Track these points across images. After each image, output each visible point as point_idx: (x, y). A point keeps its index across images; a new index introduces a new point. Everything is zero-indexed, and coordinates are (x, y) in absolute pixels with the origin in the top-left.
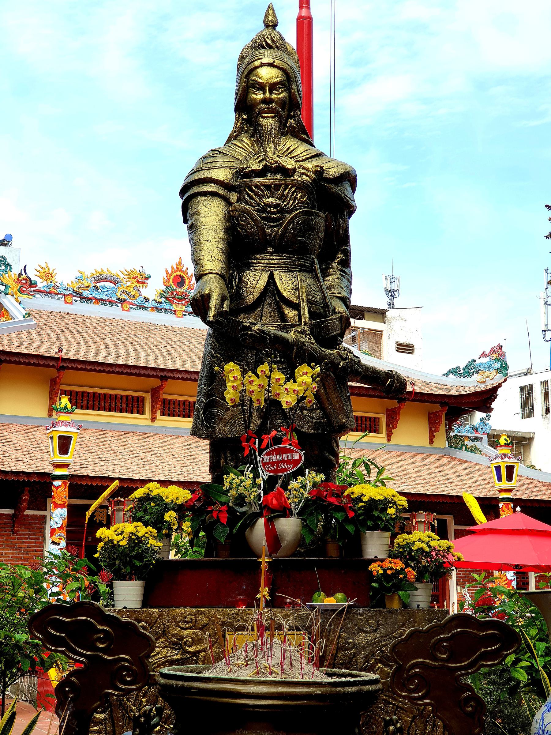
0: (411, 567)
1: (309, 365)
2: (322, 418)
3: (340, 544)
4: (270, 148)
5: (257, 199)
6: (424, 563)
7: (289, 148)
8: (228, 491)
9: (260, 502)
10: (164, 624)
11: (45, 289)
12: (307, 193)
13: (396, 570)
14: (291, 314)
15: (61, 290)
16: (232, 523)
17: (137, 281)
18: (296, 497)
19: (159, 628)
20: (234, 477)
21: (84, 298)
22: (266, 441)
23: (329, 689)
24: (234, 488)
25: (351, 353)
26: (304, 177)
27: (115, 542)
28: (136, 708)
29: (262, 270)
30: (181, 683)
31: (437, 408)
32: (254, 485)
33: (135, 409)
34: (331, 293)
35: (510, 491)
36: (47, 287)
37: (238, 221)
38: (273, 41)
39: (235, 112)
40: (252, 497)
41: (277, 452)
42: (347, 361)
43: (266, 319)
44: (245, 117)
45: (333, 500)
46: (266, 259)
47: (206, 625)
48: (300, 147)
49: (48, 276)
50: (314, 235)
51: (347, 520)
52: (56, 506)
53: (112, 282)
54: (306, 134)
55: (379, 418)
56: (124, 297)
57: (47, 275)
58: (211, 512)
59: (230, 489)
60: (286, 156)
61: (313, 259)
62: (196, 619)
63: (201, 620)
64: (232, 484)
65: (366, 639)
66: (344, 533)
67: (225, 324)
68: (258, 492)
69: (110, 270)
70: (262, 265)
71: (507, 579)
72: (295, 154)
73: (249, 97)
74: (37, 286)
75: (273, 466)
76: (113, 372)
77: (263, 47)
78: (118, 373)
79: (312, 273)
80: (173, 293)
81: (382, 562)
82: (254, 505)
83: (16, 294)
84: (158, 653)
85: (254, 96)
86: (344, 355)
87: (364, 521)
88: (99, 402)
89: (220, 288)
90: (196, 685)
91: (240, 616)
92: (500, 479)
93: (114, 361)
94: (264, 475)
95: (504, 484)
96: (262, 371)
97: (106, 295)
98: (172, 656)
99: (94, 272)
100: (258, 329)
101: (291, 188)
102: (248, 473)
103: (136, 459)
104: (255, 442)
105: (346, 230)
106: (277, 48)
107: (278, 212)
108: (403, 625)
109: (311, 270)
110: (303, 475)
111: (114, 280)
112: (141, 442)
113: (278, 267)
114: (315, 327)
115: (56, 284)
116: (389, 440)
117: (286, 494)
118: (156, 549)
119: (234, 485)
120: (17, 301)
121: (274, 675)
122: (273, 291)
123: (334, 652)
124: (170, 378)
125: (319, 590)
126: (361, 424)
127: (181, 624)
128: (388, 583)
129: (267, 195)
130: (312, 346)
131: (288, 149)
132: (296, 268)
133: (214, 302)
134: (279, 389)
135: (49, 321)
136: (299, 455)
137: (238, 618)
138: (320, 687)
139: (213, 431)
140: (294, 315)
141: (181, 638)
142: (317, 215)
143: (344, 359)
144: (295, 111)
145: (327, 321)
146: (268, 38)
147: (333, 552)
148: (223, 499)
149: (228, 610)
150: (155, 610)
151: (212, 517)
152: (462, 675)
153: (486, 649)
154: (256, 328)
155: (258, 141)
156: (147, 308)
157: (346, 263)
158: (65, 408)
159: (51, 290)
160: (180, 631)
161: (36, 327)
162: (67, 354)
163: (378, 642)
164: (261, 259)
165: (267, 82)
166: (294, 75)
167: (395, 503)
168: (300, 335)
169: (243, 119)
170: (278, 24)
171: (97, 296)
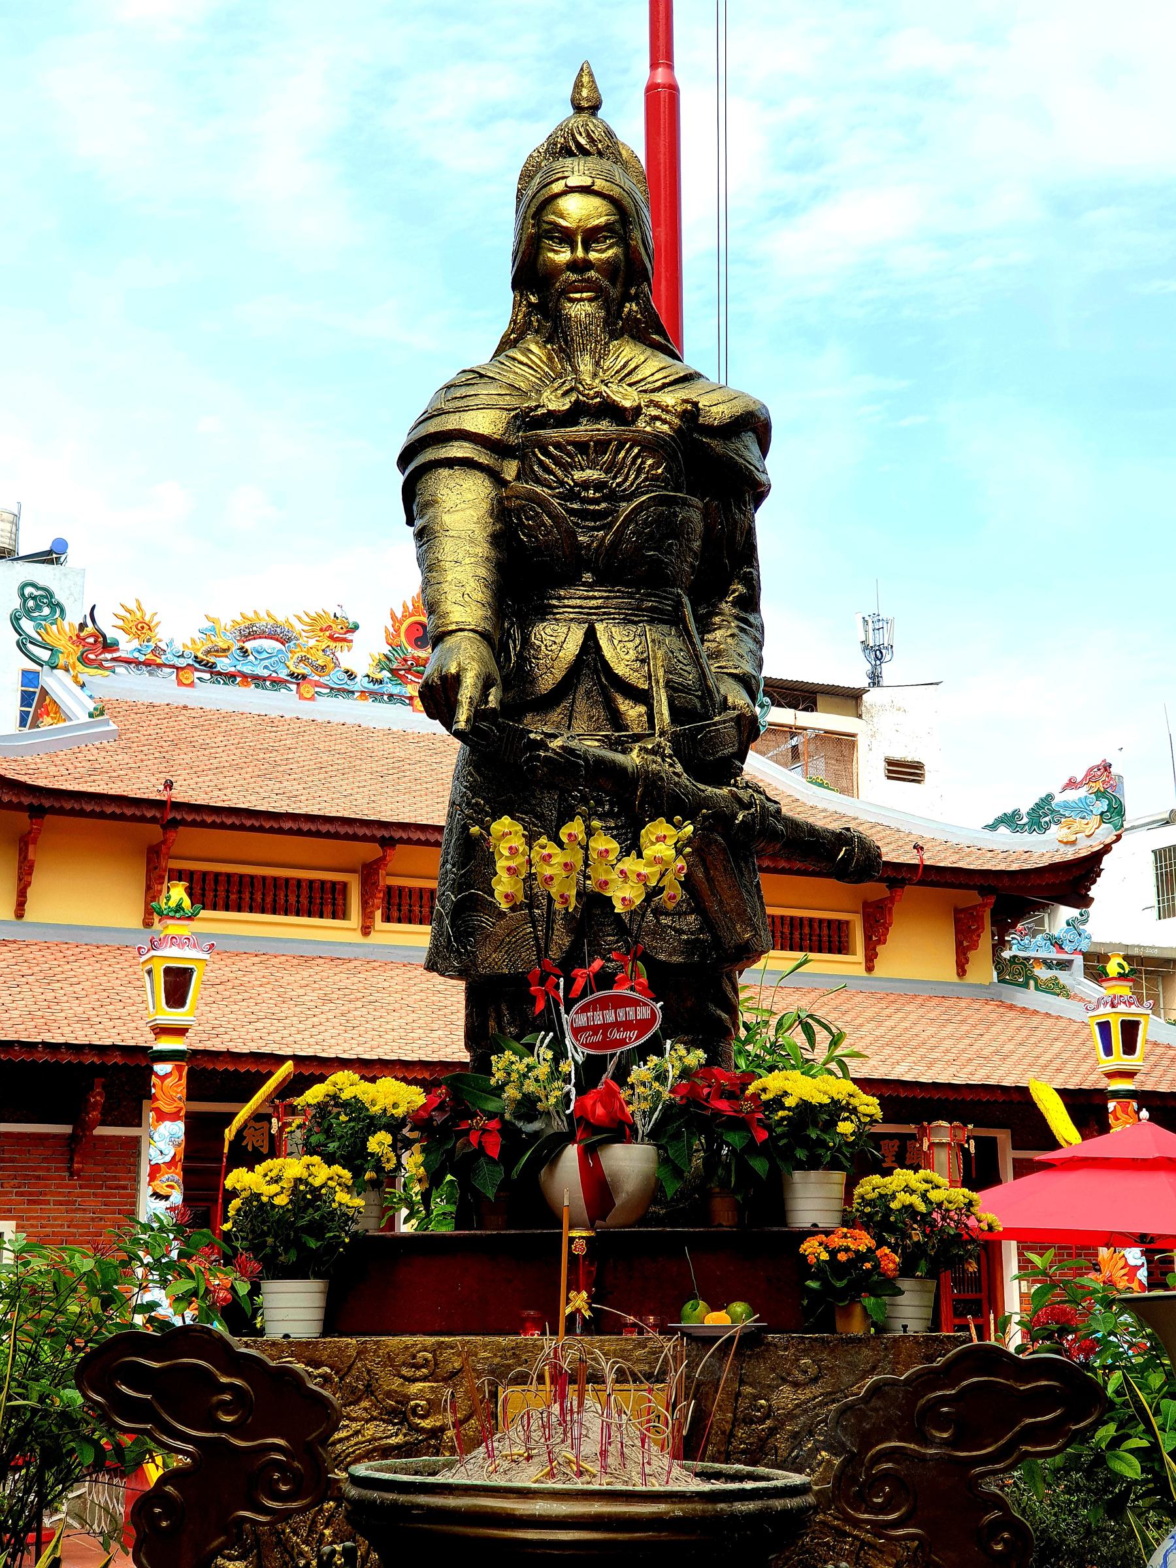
0: (889, 1245)
1: (670, 821)
2: (701, 931)
3: (739, 1198)
4: (585, 365)
5: (559, 473)
6: (917, 1236)
7: (627, 362)
8: (501, 1088)
9: (568, 1112)
10: (369, 1371)
11: (136, 655)
12: (663, 458)
13: (857, 1252)
14: (632, 712)
15: (170, 656)
16: (509, 1157)
17: (331, 637)
18: (645, 1099)
19: (357, 1379)
20: (513, 1058)
21: (219, 673)
22: (580, 983)
23: (699, 1507)
24: (514, 1082)
25: (760, 793)
26: (658, 424)
27: (265, 1199)
28: (312, 1549)
29: (572, 620)
30: (391, 1496)
31: (972, 898)
32: (555, 1074)
34: (719, 667)
35: (1129, 1075)
36: (139, 651)
37: (519, 519)
38: (592, 140)
39: (514, 287)
40: (552, 1101)
41: (603, 1004)
42: (753, 810)
43: (580, 725)
44: (533, 299)
45: (723, 1105)
46: (579, 598)
47: (457, 1373)
48: (649, 362)
49: (142, 628)
50: (681, 545)
51: (751, 1148)
52: (161, 1116)
53: (277, 640)
54: (661, 331)
55: (847, 922)
56: (302, 669)
57: (140, 625)
58: (466, 1133)
59: (505, 1084)
60: (620, 381)
61: (679, 595)
62: (435, 1360)
63: (448, 1361)
64: (509, 1074)
65: (796, 1399)
66: (746, 1172)
67: (495, 735)
68: (566, 1090)
69: (272, 612)
70: (572, 610)
71: (1126, 1265)
72: (640, 377)
73: (541, 258)
74: (118, 650)
75: (595, 1034)
76: (280, 831)
77: (571, 154)
78: (290, 832)
79: (677, 626)
80: (405, 660)
81: (827, 1236)
82: (557, 1117)
83: (74, 667)
84: (357, 1433)
85: (551, 255)
86: (746, 799)
87: (790, 1148)
88: (252, 894)
89: (481, 661)
90: (422, 1499)
91: (528, 1352)
92: (1108, 1051)
93: (282, 806)
94: (576, 1053)
95: (1119, 1060)
96: (570, 835)
97: (266, 667)
98: (386, 1437)
99: (239, 619)
100: (562, 747)
101: (631, 448)
102: (542, 1050)
103: (330, 1015)
104: (558, 984)
105: (750, 532)
106: (600, 154)
107: (604, 499)
108: (874, 1368)
109: (674, 620)
110: (660, 1053)
112: (339, 978)
113: (605, 614)
114: (683, 740)
115: (160, 644)
116: (870, 969)
117: (624, 1094)
118: (351, 1212)
119: (514, 1076)
120: (77, 682)
121: (587, 1478)
122: (596, 665)
123: (728, 1427)
124: (401, 841)
125: (695, 1298)
126: (811, 935)
127: (405, 1371)
128: (841, 1280)
129: (580, 465)
130: (677, 779)
131: (624, 366)
132: (644, 616)
133: (468, 690)
134: (607, 872)
135: (144, 724)
136: (652, 1009)
137: (524, 1357)
138: (680, 1502)
139: (471, 961)
140: (640, 716)
141: (405, 1399)
142: (684, 503)
143: (747, 806)
144: (639, 286)
145: (709, 725)
146: (581, 135)
147: (724, 1216)
148: (492, 1106)
149: (503, 1341)
150: (349, 1340)
151: (468, 1143)
152: (983, 1475)
153: (1033, 1420)
154: (556, 744)
155: (561, 350)
156: (353, 692)
157: (750, 603)
158: (179, 908)
159: (147, 657)
160: (402, 1384)
161: (118, 736)
162: (180, 794)
163: (822, 1404)
164: (568, 599)
165: (579, 227)
166: (636, 209)
167: (854, 1111)
168: (651, 757)
169: (530, 304)
170: (601, 103)
171: (247, 669)
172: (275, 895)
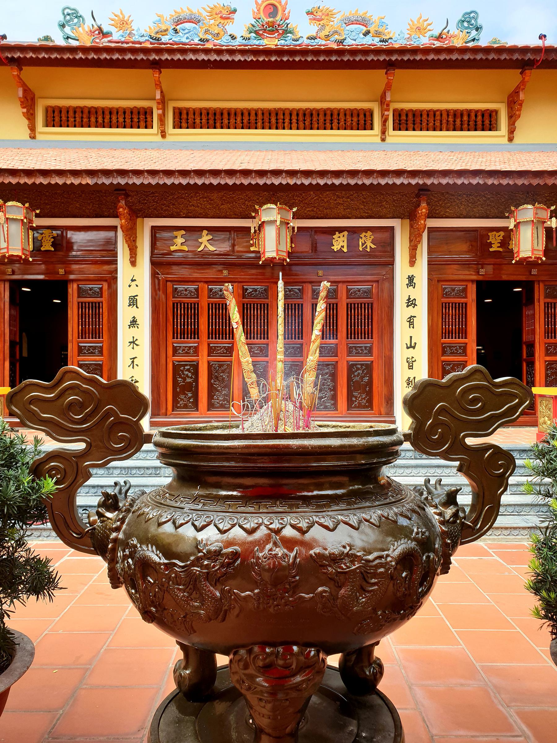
17: (221, 17)
33: (142, 124)
36: (122, 36)
53: (193, 22)
69: (190, 8)
97: (187, 38)
99: (174, 14)
111: (196, 21)
126: (469, 121)
172: (110, 118)
